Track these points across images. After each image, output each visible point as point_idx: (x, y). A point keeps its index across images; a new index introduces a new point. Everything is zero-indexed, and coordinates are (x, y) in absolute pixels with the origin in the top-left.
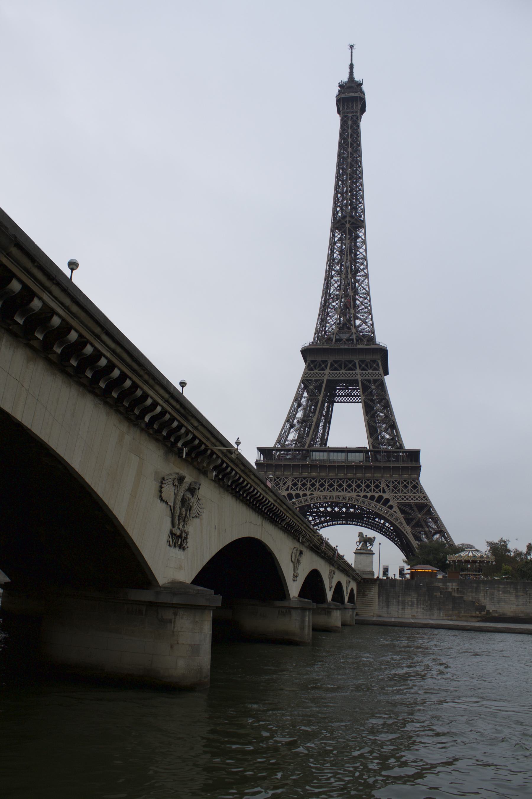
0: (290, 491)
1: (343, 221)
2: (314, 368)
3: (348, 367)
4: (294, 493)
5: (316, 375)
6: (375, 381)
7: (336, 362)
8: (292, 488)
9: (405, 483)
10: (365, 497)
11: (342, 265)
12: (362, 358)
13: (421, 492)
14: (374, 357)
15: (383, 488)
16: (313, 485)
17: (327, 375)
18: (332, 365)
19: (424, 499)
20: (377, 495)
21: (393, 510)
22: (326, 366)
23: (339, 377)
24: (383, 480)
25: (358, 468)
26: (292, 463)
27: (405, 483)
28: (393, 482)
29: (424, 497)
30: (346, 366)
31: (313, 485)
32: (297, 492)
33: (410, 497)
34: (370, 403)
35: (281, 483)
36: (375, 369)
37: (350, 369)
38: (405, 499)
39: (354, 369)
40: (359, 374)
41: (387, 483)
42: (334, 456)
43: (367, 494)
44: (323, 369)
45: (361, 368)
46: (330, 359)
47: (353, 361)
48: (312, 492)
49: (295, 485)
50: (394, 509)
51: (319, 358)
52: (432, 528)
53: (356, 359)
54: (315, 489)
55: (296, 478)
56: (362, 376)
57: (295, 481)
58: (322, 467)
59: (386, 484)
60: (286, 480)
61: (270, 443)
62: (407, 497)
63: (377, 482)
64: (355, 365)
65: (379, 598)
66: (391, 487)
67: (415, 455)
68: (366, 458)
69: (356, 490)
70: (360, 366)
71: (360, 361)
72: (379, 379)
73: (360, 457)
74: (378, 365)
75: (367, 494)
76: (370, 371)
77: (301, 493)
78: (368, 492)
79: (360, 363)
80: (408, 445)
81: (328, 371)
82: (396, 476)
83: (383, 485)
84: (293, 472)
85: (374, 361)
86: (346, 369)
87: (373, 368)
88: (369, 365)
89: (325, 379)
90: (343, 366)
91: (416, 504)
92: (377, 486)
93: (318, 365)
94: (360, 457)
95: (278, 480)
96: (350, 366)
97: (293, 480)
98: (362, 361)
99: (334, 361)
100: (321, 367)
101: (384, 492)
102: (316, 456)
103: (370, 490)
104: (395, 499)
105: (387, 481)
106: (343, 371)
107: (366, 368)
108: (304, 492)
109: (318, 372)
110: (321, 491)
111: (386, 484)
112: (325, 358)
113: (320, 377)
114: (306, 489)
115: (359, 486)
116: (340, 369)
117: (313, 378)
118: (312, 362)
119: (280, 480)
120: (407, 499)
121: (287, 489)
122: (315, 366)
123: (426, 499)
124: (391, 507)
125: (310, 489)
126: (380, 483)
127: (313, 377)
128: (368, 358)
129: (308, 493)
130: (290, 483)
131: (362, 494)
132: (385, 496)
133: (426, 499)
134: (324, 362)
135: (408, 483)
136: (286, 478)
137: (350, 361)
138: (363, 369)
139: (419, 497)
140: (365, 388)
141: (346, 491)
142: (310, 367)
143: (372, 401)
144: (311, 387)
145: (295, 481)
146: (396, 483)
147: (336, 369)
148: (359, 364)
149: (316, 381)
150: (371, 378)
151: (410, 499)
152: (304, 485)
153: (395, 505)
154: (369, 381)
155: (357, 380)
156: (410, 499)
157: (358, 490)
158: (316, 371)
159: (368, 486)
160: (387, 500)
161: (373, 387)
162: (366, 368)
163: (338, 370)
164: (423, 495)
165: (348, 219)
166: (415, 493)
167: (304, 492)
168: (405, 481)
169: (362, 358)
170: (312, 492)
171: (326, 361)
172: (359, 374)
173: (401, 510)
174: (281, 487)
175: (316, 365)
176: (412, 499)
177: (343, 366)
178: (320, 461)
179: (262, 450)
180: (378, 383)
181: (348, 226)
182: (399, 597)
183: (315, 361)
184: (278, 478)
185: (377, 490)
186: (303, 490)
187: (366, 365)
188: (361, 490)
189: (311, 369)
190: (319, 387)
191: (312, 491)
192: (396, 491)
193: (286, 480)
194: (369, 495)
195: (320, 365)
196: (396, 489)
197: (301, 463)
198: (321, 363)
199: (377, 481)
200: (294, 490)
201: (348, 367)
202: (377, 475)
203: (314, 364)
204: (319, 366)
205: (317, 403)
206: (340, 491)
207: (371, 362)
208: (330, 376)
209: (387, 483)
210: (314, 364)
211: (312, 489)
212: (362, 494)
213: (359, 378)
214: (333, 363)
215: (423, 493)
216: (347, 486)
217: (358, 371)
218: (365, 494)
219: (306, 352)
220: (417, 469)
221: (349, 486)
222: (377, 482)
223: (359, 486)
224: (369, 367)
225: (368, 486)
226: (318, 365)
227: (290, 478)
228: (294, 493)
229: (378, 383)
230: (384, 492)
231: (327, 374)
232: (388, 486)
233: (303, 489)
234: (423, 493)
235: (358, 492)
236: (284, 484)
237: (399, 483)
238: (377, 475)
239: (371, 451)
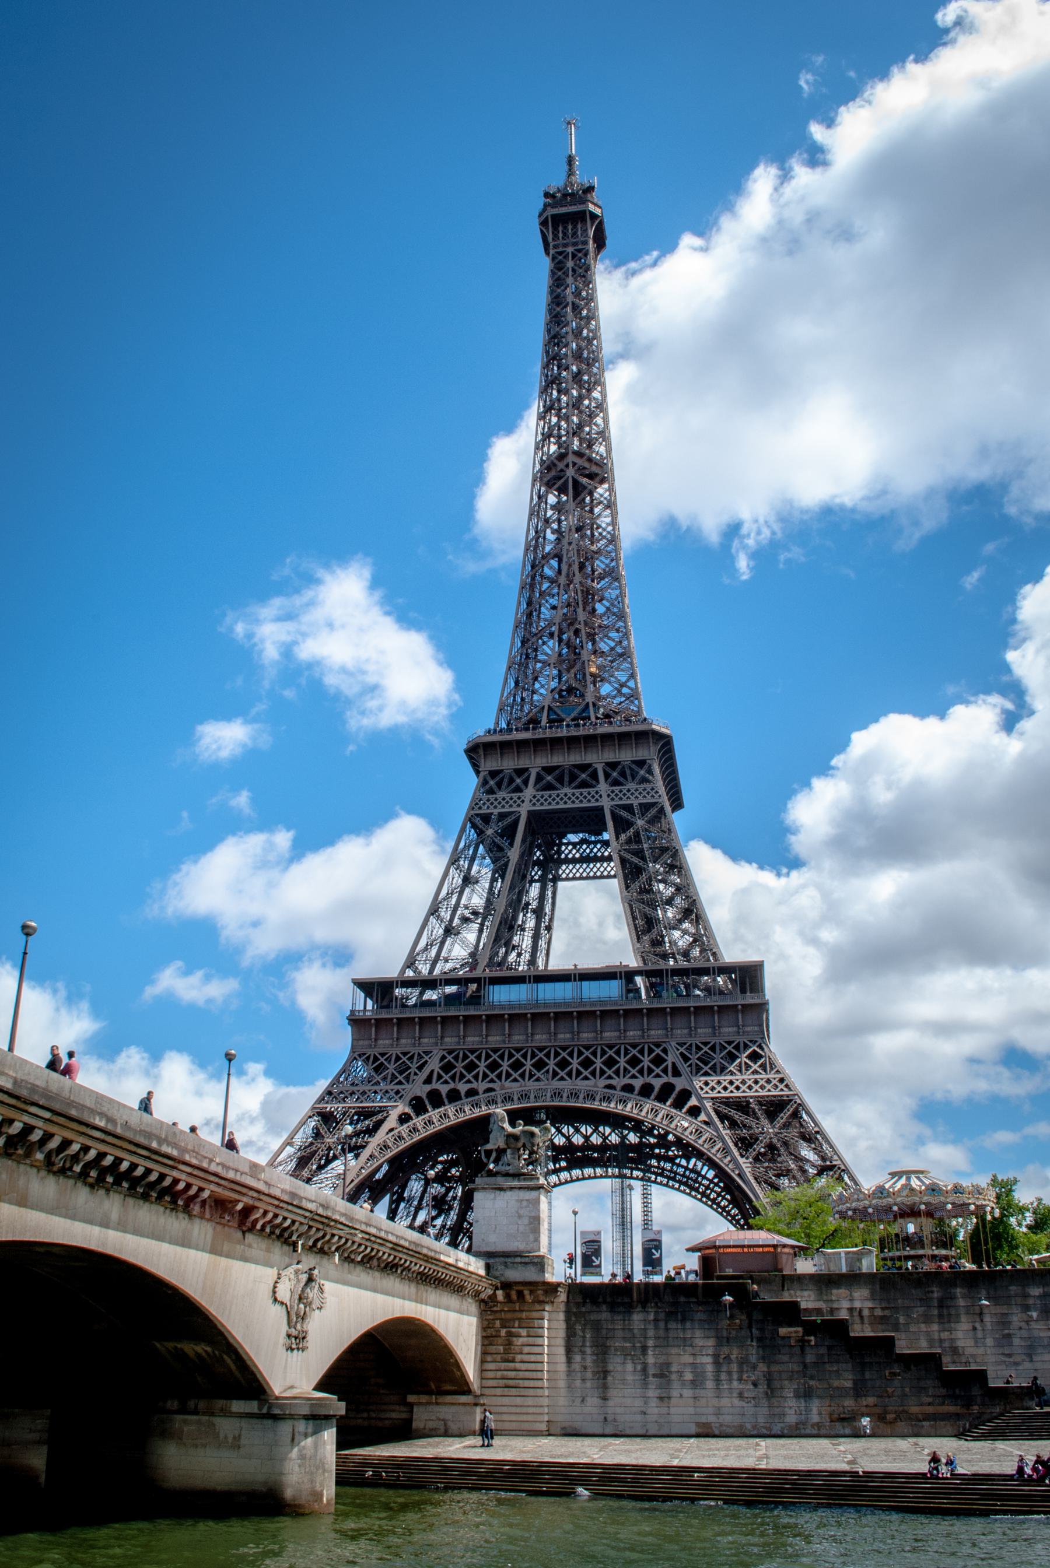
0: (435, 1085)
1: (561, 465)
2: (495, 788)
3: (579, 780)
4: (444, 1089)
5: (502, 802)
6: (645, 807)
7: (548, 770)
8: (440, 1077)
9: (730, 1048)
10: (628, 1088)
11: (560, 562)
12: (610, 756)
13: (772, 1069)
14: (641, 754)
15: (674, 1064)
16: (494, 1066)
17: (528, 802)
18: (539, 778)
19: (781, 1086)
20: (657, 1083)
21: (699, 1119)
22: (526, 782)
23: (558, 803)
24: (673, 1044)
25: (607, 1014)
26: (440, 1012)
27: (730, 1048)
28: (699, 1048)
29: (782, 1080)
30: (573, 777)
31: (494, 1066)
32: (452, 1085)
33: (744, 1082)
34: (635, 860)
35: (414, 1069)
36: (644, 780)
37: (584, 785)
38: (731, 1088)
39: (594, 783)
40: (605, 796)
41: (682, 1050)
42: (550, 992)
43: (633, 1082)
44: (518, 789)
45: (609, 780)
46: (535, 763)
47: (590, 765)
48: (491, 1085)
49: (447, 1067)
50: (703, 1117)
51: (508, 764)
52: (808, 1161)
53: (597, 758)
54: (499, 1076)
55: (450, 1052)
56: (613, 799)
57: (450, 1058)
58: (515, 1018)
59: (682, 1054)
60: (426, 1058)
61: (388, 966)
62: (737, 1083)
63: (658, 1051)
64: (594, 775)
65: (569, 1361)
66: (694, 1059)
67: (749, 976)
68: (629, 991)
69: (603, 1072)
70: (607, 776)
71: (607, 764)
72: (654, 804)
73: (612, 990)
74: (650, 772)
75: (633, 1082)
76: (632, 786)
77: (463, 1088)
78: (634, 1077)
79: (608, 769)
80: (733, 952)
81: (529, 792)
82: (703, 1033)
83: (670, 1059)
84: (442, 1037)
85: (641, 763)
86: (573, 785)
87: (638, 778)
88: (628, 772)
89: (523, 811)
90: (566, 779)
91: (760, 1101)
92: (658, 1061)
93: (506, 780)
94: (612, 990)
95: (404, 1059)
96: (582, 776)
97: (443, 1058)
98: (613, 765)
99: (544, 769)
100: (514, 785)
101: (676, 1073)
102: (502, 995)
103: (641, 1072)
104: (706, 1089)
105: (681, 1044)
106: (566, 790)
107: (622, 780)
108: (469, 1086)
109: (507, 796)
110: (515, 1080)
111: (682, 1054)
112: (523, 763)
113: (511, 806)
114: (476, 1077)
115: (610, 1063)
116: (558, 785)
117: (496, 812)
118: (493, 774)
119: (411, 1058)
120: (738, 1088)
121: (428, 1081)
122: (499, 785)
123: (787, 1086)
124: (694, 1112)
125: (485, 1076)
126: (665, 1051)
127: (495, 807)
128: (626, 755)
129: (482, 1086)
130: (434, 1065)
131: (619, 1082)
132: (680, 1084)
133: (787, 1086)
134: (520, 772)
135: (737, 1047)
136: (427, 1053)
137: (584, 768)
138: (616, 783)
139: (768, 1081)
140: (622, 825)
141: (577, 1076)
142: (487, 787)
143: (640, 854)
144: (490, 832)
145: (450, 1058)
146: (706, 1049)
147: (549, 787)
148: (605, 772)
149: (502, 816)
150: (636, 803)
151: (744, 1088)
152: (471, 1067)
153: (708, 1105)
154: (629, 808)
155: (601, 809)
156: (744, 1088)
157: (610, 1072)
158: (501, 795)
159: (634, 1062)
160: (685, 1095)
161: (640, 823)
162: (622, 780)
163: (556, 789)
164: (780, 1076)
165: (571, 458)
166: (755, 1072)
167: (469, 1086)
168: (729, 1043)
169: (610, 756)
170: (491, 1085)
171: (527, 769)
172: (605, 796)
173: (722, 1117)
174: (412, 1077)
175: (502, 780)
176: (750, 1088)
177: (566, 779)
178: (511, 1006)
179: (367, 987)
180: (653, 811)
181: (570, 472)
182: (644, 1349)
183: (501, 771)
184: (405, 1054)
185: (658, 1071)
186: (469, 1081)
187: (623, 774)
188: (617, 1072)
189: (491, 791)
190: (509, 832)
191: (492, 1081)
192: (706, 1068)
193: (426, 1058)
194: (637, 1083)
195: (511, 781)
196: (706, 1064)
197: (462, 1012)
198: (515, 776)
199: (658, 1045)
200: (446, 1082)
201: (579, 780)
202: (656, 1034)
203: (498, 779)
204: (508, 785)
205: (506, 865)
206: (562, 1079)
207: (633, 766)
208: (534, 804)
209: (682, 1050)
210: (498, 779)
211: (492, 1076)
212: (619, 1082)
213: (606, 804)
214: (543, 773)
215: (778, 1072)
216: (580, 1064)
217: (603, 787)
218: (627, 1081)
219: (476, 751)
220: (758, 1011)
221: (587, 1063)
222: (658, 1051)
223: (610, 1063)
224: (629, 778)
225: (634, 1062)
226: (506, 780)
227: (435, 1052)
228: (444, 1089)
229: (653, 811)
230: (676, 1073)
231: (527, 800)
232: (686, 1059)
233: (469, 1077)
234: (778, 1072)
235: (610, 1077)
236: (420, 1068)
237: (713, 1049)
238: (656, 1034)
239: (639, 973)
